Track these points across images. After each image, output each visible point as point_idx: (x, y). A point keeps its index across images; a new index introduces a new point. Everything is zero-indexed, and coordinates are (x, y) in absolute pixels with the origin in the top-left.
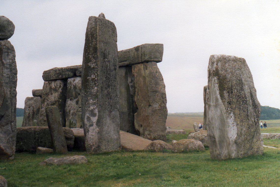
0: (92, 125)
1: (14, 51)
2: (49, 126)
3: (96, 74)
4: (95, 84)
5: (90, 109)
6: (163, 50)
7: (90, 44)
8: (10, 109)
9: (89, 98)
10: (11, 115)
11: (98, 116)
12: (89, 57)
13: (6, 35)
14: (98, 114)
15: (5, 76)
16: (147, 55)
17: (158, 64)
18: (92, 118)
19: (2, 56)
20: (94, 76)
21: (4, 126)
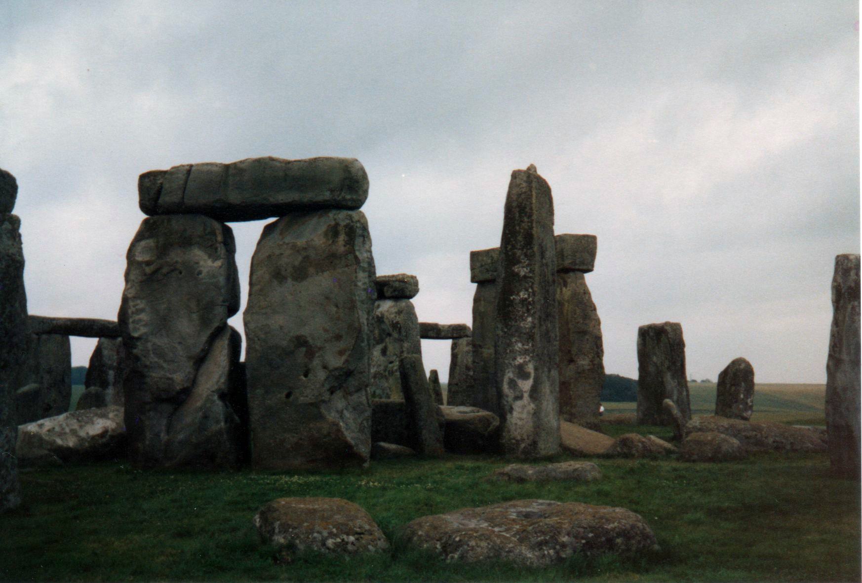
0: (519, 397)
4: (528, 310)
5: (517, 363)
6: (596, 248)
7: (517, 228)
9: (514, 340)
12: (514, 254)
14: (532, 375)
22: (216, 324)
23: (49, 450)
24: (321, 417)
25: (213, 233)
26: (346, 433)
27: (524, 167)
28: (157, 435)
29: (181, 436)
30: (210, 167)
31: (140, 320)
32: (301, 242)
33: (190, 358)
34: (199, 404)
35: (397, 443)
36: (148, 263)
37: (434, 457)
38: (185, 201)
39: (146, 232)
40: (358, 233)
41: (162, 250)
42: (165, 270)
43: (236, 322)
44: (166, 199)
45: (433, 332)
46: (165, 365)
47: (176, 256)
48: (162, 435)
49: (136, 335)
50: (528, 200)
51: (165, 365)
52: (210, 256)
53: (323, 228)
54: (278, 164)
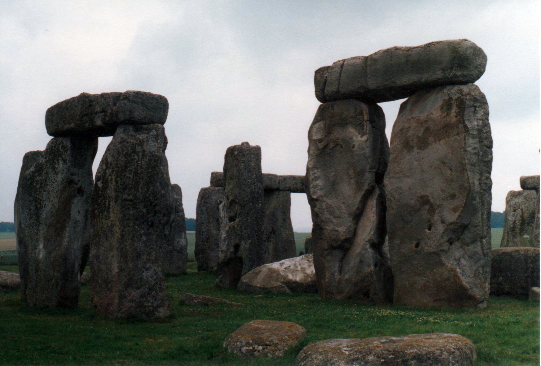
1: (486, 103)
8: (480, 213)
10: (481, 224)
13: (472, 75)
15: (470, 152)
19: (463, 115)
21: (468, 245)
23: (283, 283)
24: (442, 264)
26: (462, 278)
28: (333, 274)
29: (347, 276)
30: (354, 61)
31: (317, 185)
32: (423, 116)
33: (350, 214)
34: (358, 251)
36: (320, 141)
38: (340, 89)
39: (321, 115)
41: (328, 130)
42: (331, 145)
46: (334, 220)
47: (338, 134)
48: (336, 274)
51: (334, 220)
52: (359, 133)
53: (440, 103)
54: (401, 52)
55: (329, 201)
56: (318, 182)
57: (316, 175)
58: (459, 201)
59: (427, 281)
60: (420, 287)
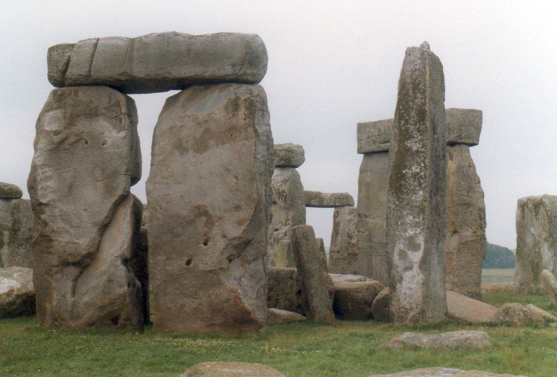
0: (409, 268)
2: (300, 266)
3: (422, 165)
4: (420, 184)
5: (408, 235)
6: (481, 122)
7: (411, 104)
8: (264, 227)
9: (405, 213)
10: (264, 240)
11: (424, 250)
12: (407, 130)
14: (422, 247)
15: (259, 159)
16: (455, 131)
17: (471, 149)
18: (410, 253)
19: (254, 117)
20: (417, 168)
21: (249, 264)
22: (119, 192)
24: (220, 284)
25: (118, 105)
26: (244, 300)
27: (418, 45)
28: (64, 296)
29: (86, 299)
30: (115, 41)
31: (48, 187)
32: (202, 115)
33: (95, 224)
34: (103, 268)
35: (285, 308)
36: (56, 133)
37: (324, 323)
38: (92, 73)
40: (257, 108)
41: (71, 121)
43: (139, 191)
44: (73, 72)
45: (317, 200)
46: (71, 231)
47: (83, 126)
48: (69, 296)
49: (44, 201)
50: (422, 78)
51: (71, 231)
52: (115, 127)
53: (225, 102)
54: (181, 38)
55: (65, 208)
56: (49, 183)
57: (46, 174)
58: (247, 213)
59: (200, 304)
60: (190, 311)
